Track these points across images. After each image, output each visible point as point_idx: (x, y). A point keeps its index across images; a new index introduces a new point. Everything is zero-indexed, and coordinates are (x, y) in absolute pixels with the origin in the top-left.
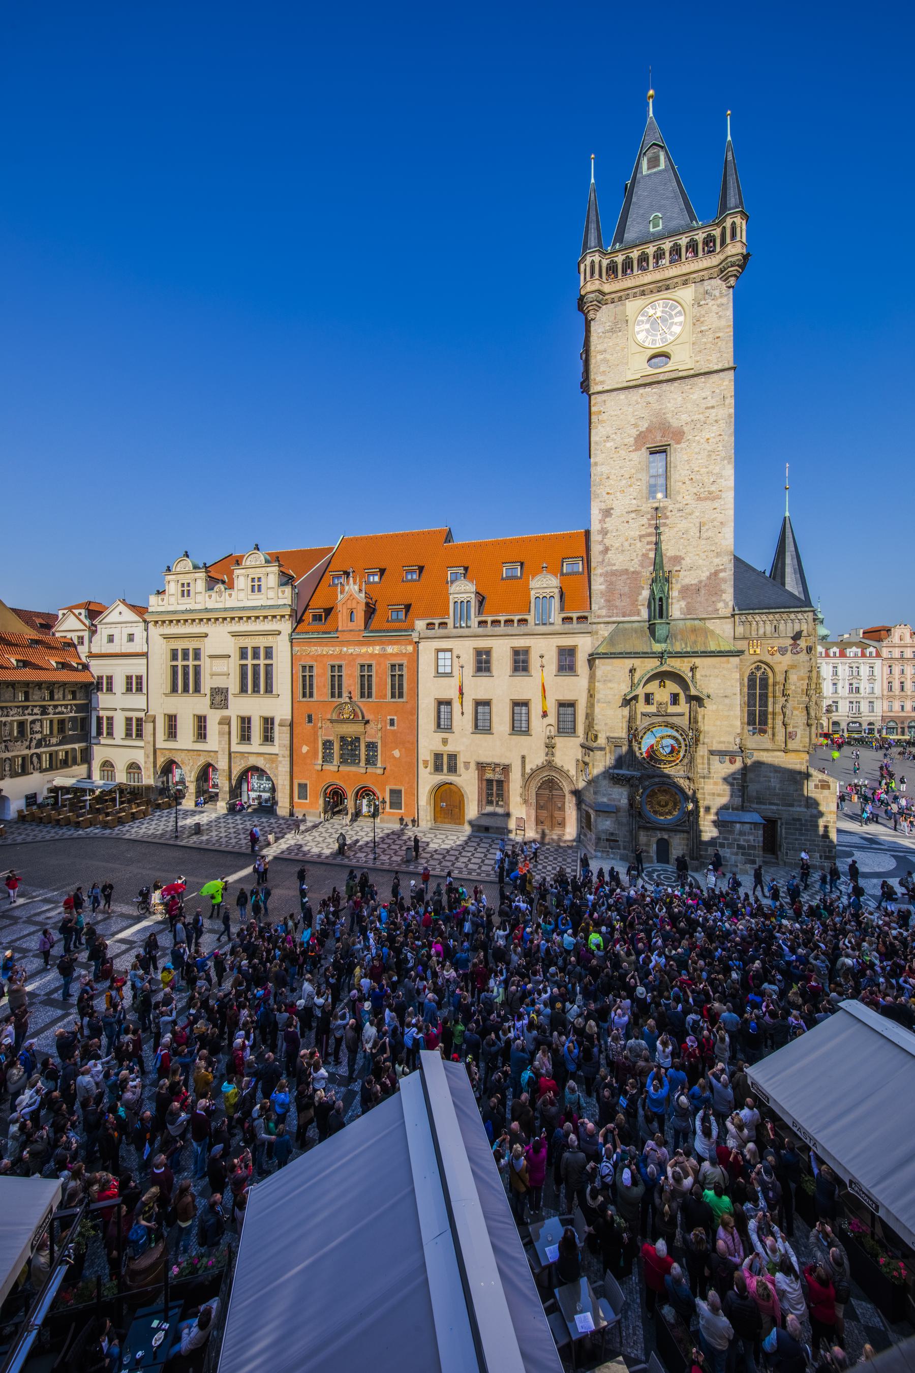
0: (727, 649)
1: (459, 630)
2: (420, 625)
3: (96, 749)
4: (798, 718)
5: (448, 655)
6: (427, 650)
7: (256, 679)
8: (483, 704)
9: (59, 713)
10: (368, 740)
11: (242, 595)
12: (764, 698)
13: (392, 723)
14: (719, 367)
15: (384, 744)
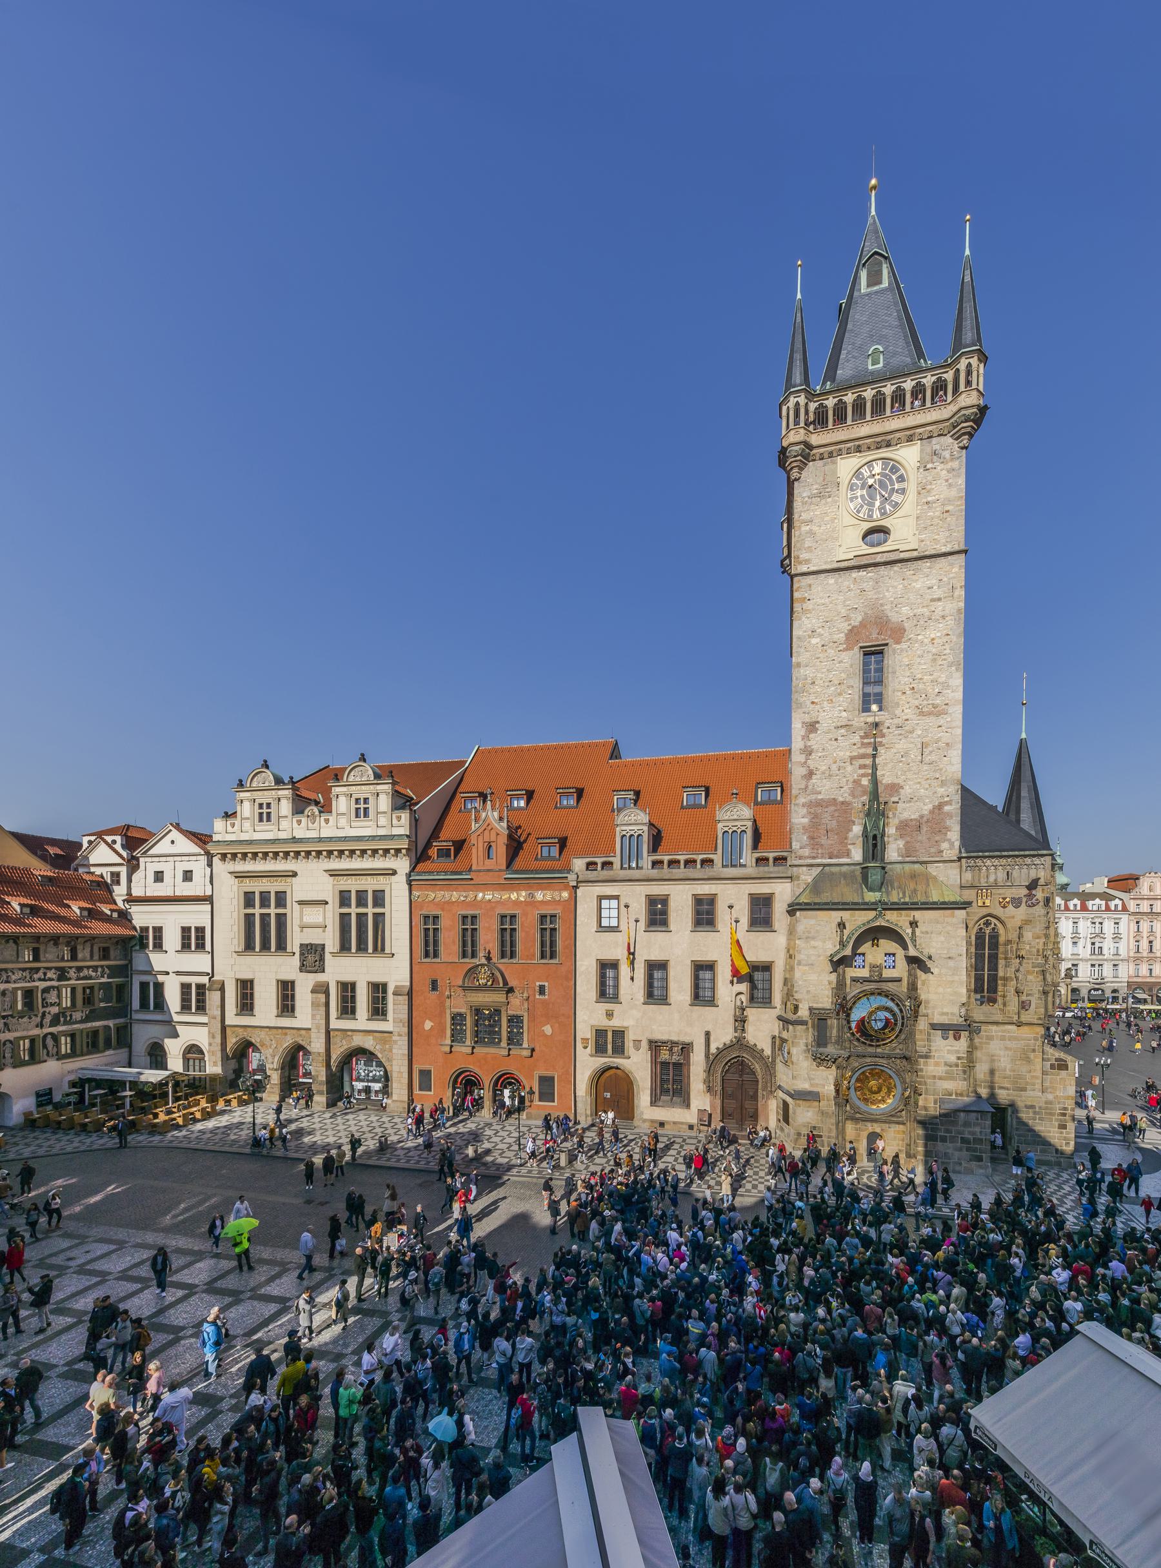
0: (953, 900)
1: (628, 872)
2: (579, 864)
3: (136, 1028)
4: (1033, 984)
5: (614, 903)
6: (587, 896)
7: (361, 932)
8: (657, 968)
9: (85, 978)
10: (510, 1012)
11: (343, 821)
12: (994, 959)
13: (542, 990)
14: (948, 549)
15: (532, 1018)
